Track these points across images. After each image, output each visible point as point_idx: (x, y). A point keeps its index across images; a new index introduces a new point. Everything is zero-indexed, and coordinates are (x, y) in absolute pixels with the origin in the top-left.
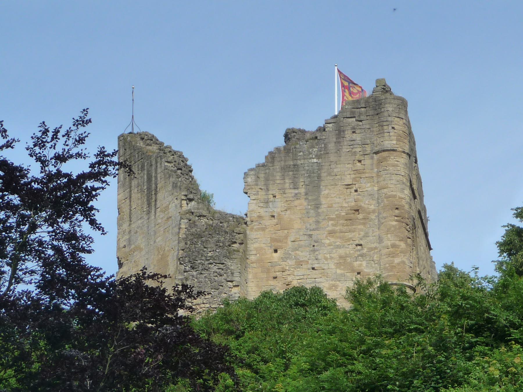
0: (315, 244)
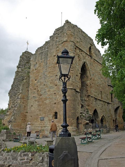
0: (45, 77)
